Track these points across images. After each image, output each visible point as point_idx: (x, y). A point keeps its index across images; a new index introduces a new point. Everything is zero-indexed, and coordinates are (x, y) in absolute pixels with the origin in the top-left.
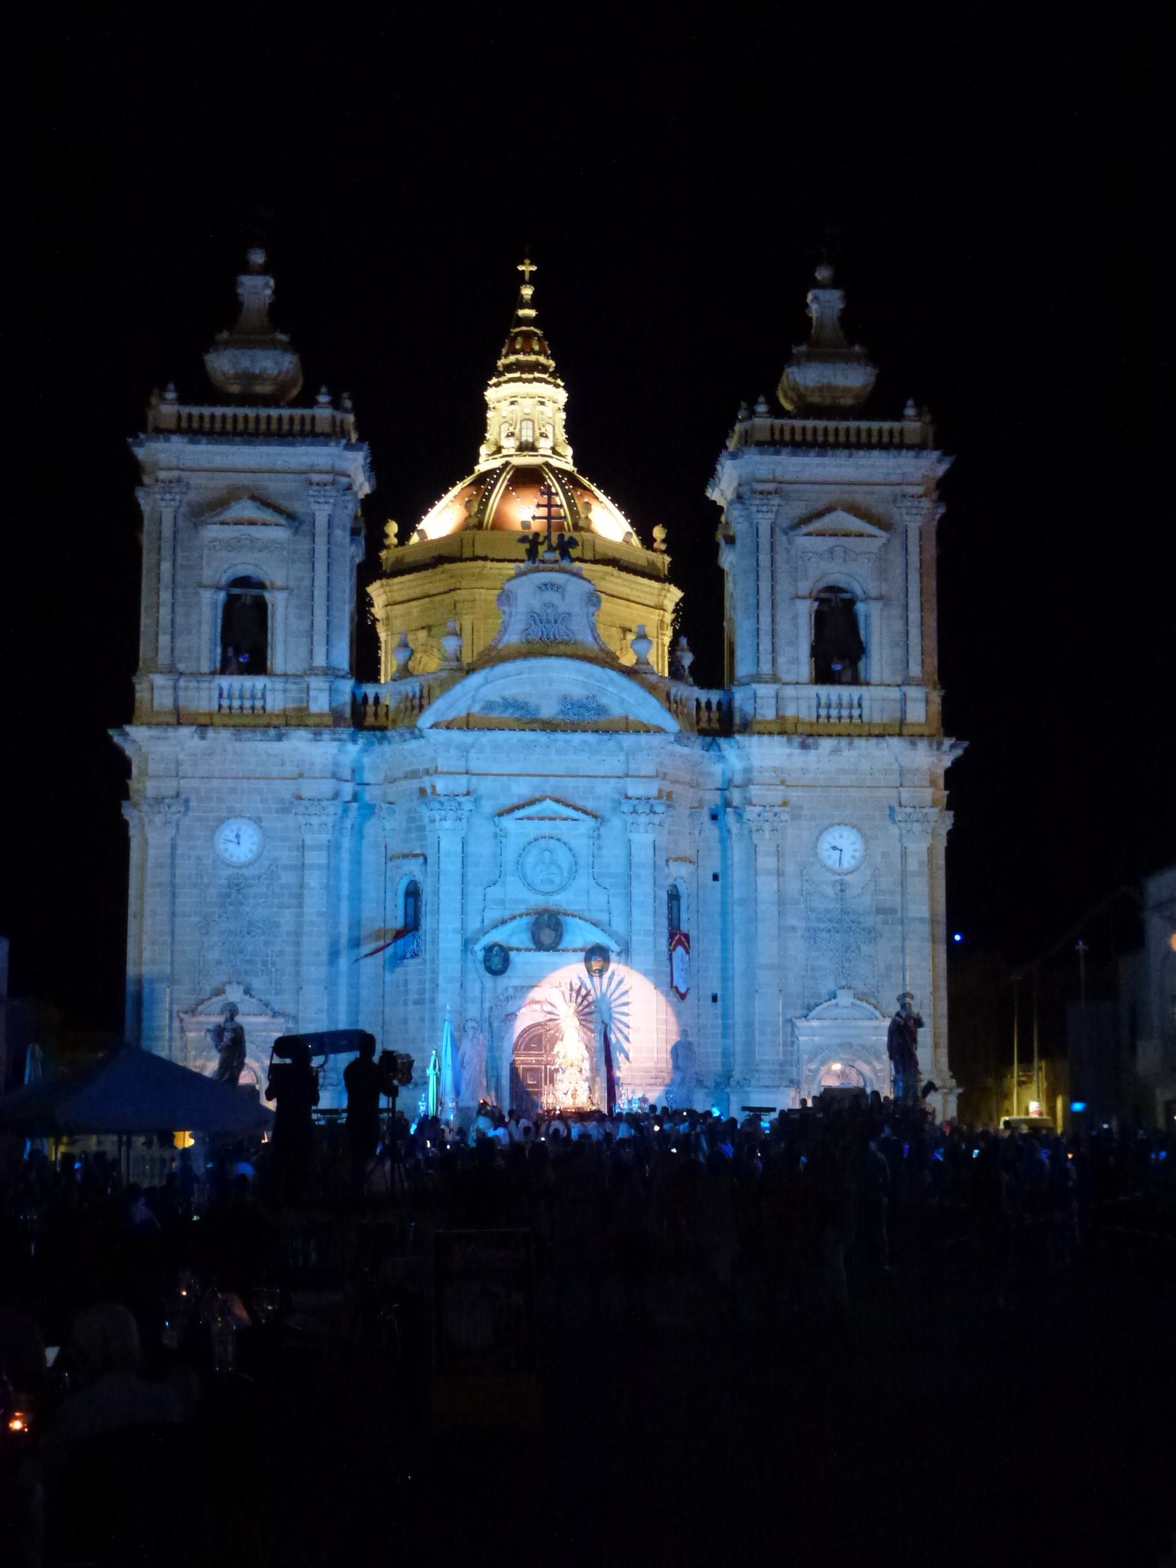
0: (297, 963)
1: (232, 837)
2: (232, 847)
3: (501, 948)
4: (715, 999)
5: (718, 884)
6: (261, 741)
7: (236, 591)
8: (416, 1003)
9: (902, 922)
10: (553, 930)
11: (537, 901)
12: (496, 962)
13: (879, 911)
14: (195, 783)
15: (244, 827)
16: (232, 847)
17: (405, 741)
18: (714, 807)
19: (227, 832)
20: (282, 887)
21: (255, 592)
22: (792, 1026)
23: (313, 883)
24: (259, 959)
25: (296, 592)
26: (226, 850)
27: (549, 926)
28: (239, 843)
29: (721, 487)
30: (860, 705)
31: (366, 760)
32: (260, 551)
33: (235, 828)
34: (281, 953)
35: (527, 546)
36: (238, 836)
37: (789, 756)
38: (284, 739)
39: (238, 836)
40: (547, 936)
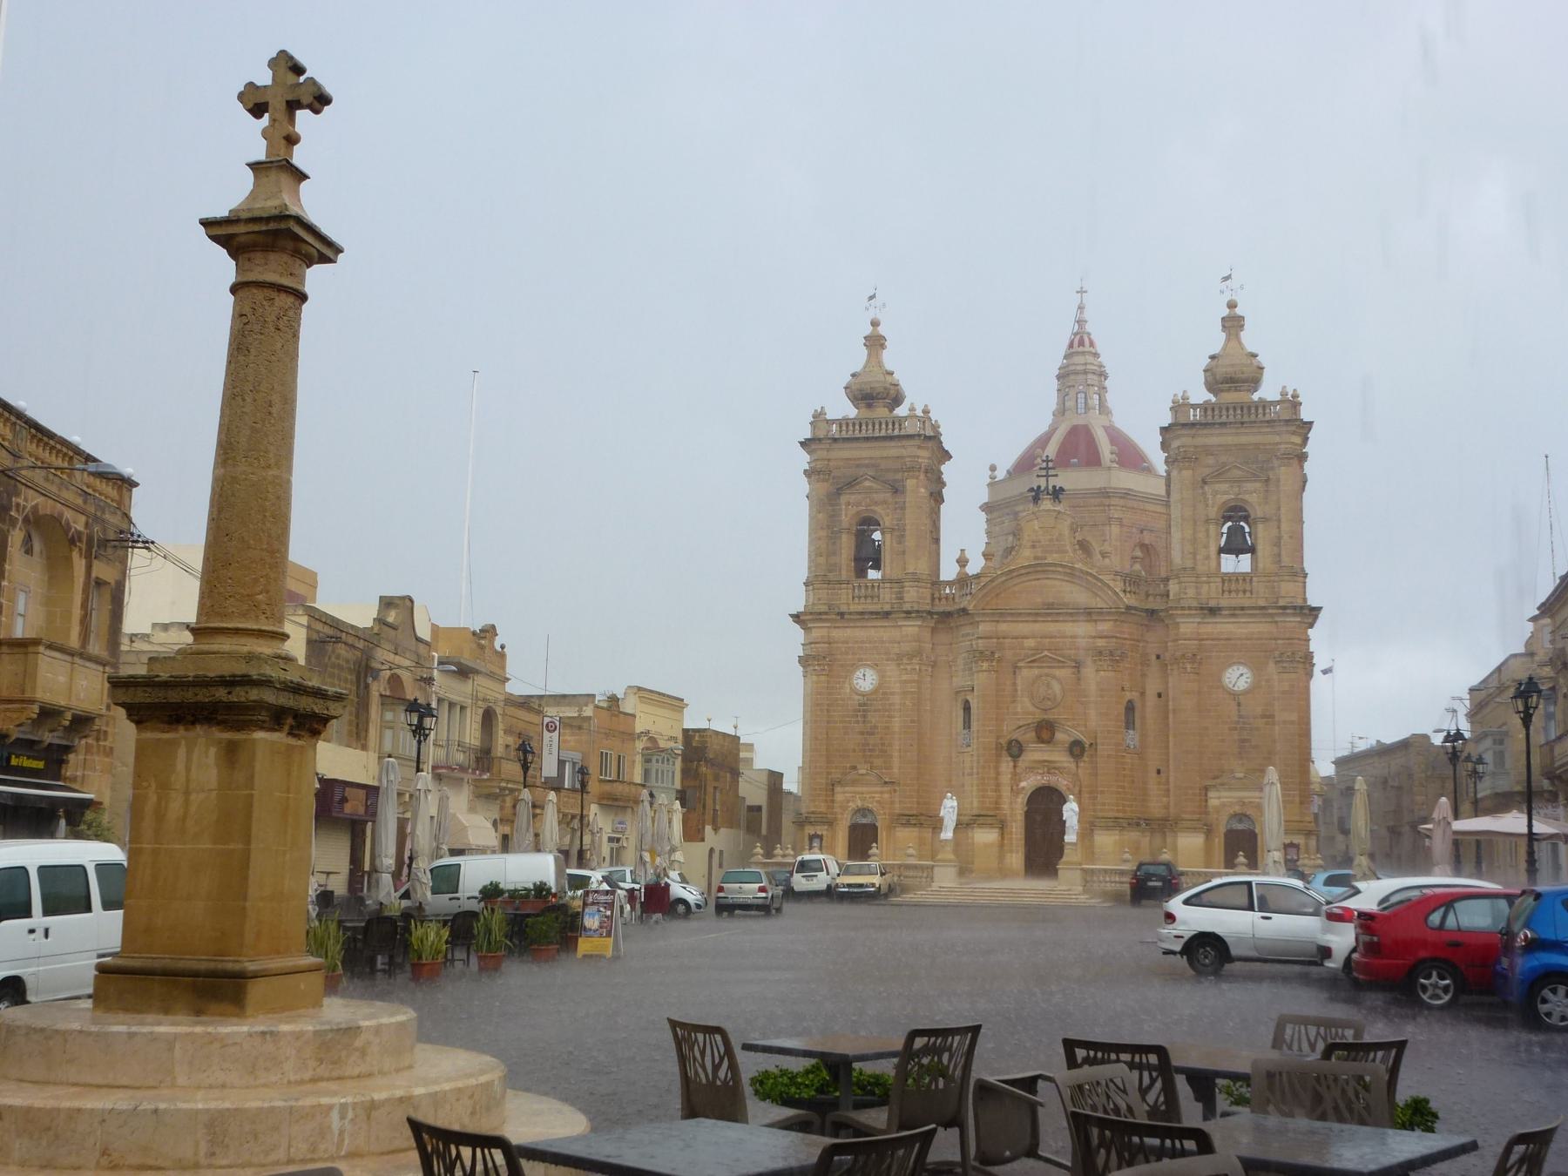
2: (860, 681)
4: (1159, 772)
8: (968, 775)
12: (1015, 750)
13: (1264, 716)
16: (860, 681)
19: (858, 673)
26: (857, 684)
35: (1033, 494)
36: (864, 675)
39: (864, 675)
40: (1045, 735)
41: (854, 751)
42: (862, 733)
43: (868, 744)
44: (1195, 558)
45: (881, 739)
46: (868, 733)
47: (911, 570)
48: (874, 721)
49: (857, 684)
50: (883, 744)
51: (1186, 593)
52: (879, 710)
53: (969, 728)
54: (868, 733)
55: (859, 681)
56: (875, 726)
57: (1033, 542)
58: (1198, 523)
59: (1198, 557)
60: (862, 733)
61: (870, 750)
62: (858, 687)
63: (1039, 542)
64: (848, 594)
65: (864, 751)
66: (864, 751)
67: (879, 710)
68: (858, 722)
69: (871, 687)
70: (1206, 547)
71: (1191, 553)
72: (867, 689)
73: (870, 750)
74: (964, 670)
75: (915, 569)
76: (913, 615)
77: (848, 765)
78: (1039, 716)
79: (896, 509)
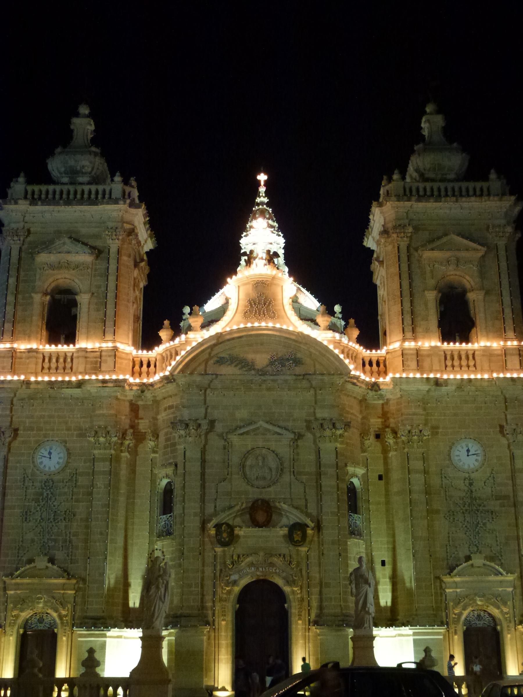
0: (86, 541)
1: (46, 454)
2: (46, 461)
3: (228, 525)
4: (383, 563)
5: (382, 482)
7: (58, 297)
9: (515, 506)
11: (254, 494)
13: (498, 498)
15: (54, 447)
16: (46, 461)
18: (377, 429)
19: (43, 451)
21: (70, 297)
22: (440, 583)
24: (61, 538)
25: (95, 294)
26: (41, 463)
28: (50, 458)
29: (373, 235)
30: (474, 358)
32: (74, 269)
33: (48, 448)
34: (76, 535)
36: (50, 453)
38: (82, 386)
39: (50, 453)
40: (261, 517)
49: (41, 463)
55: (44, 459)
62: (42, 466)
64: (36, 364)
69: (57, 466)
74: (166, 447)
76: (110, 385)
79: (95, 276)
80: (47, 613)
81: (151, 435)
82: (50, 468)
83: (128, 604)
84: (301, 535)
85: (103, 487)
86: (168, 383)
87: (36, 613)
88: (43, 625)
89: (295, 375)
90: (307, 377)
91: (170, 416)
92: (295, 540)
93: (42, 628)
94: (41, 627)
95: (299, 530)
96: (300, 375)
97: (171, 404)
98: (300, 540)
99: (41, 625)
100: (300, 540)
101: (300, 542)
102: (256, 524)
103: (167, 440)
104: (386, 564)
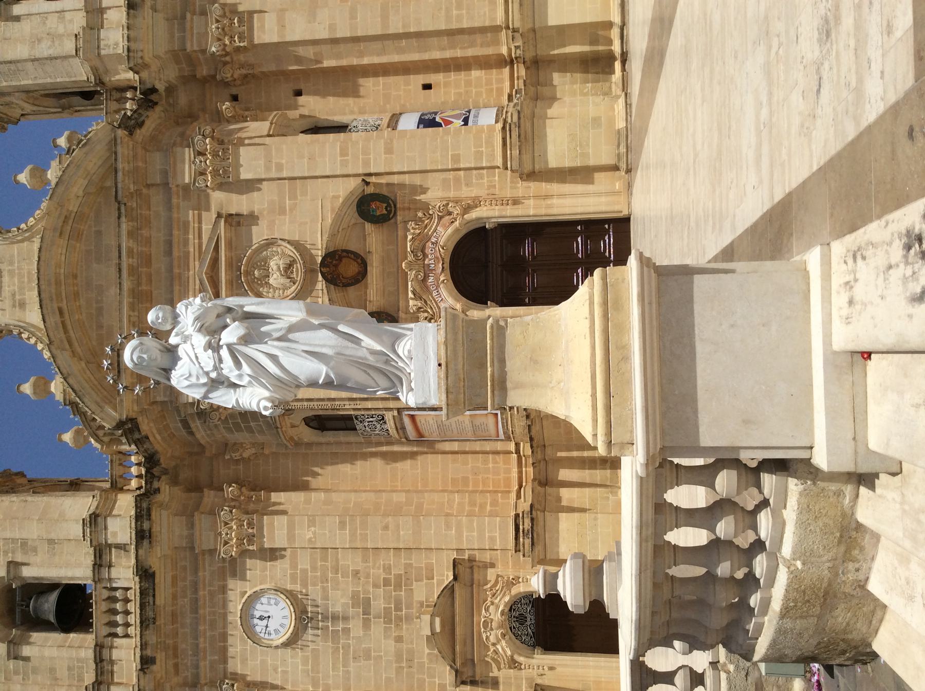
1: (265, 622)
2: (273, 624)
4: (427, 87)
6: (154, 596)
10: (341, 261)
14: (204, 665)
17: (147, 437)
20: (314, 569)
23: (310, 535)
27: (336, 266)
28: (269, 617)
31: (185, 474)
33: (256, 621)
34: (387, 569)
36: (261, 618)
37: (154, 9)
38: (151, 571)
39: (261, 618)
40: (349, 268)
41: (399, 639)
42: (366, 624)
43: (387, 611)
44: (61, 36)
45: (376, 586)
46: (366, 612)
47: (76, 530)
48: (343, 601)
50: (387, 582)
51: (117, 44)
52: (324, 589)
53: (349, 418)
54: (366, 612)
56: (353, 597)
57: (14, 306)
58: (8, 35)
59: (61, 30)
60: (366, 624)
61: (398, 608)
63: (14, 295)
65: (399, 619)
66: (399, 619)
67: (324, 589)
68: (346, 631)
69: (282, 604)
70: (44, 15)
71: (53, 42)
72: (287, 612)
73: (398, 608)
74: (250, 430)
75: (77, 521)
77: (427, 651)
78: (321, 284)
80: (510, 610)
81: (233, 455)
82: (284, 617)
83: (277, 490)
84: (378, 203)
85: (313, 529)
86: (139, 431)
87: (511, 628)
88: (528, 616)
89: (119, 218)
90: (120, 198)
91: (199, 424)
92: (386, 212)
93: (533, 617)
94: (530, 619)
95: (369, 205)
96: (119, 209)
97: (180, 425)
98: (385, 205)
99: (529, 619)
100: (385, 205)
101: (389, 205)
102: (362, 275)
103: (238, 428)
104: (427, 82)
